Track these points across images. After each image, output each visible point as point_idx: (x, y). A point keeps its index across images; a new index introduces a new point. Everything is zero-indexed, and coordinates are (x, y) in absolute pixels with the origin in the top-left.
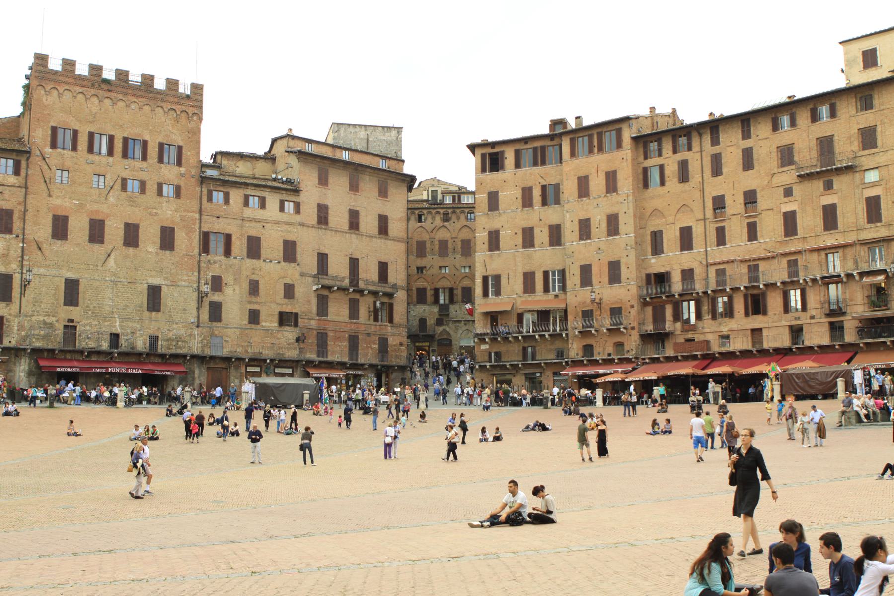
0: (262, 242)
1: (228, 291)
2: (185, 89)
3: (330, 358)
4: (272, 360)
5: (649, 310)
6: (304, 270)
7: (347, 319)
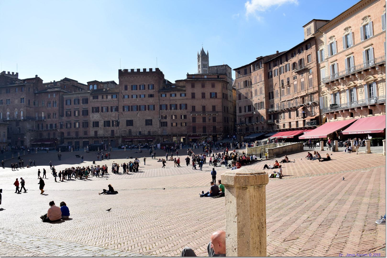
1: (167, 118)
2: (154, 70)
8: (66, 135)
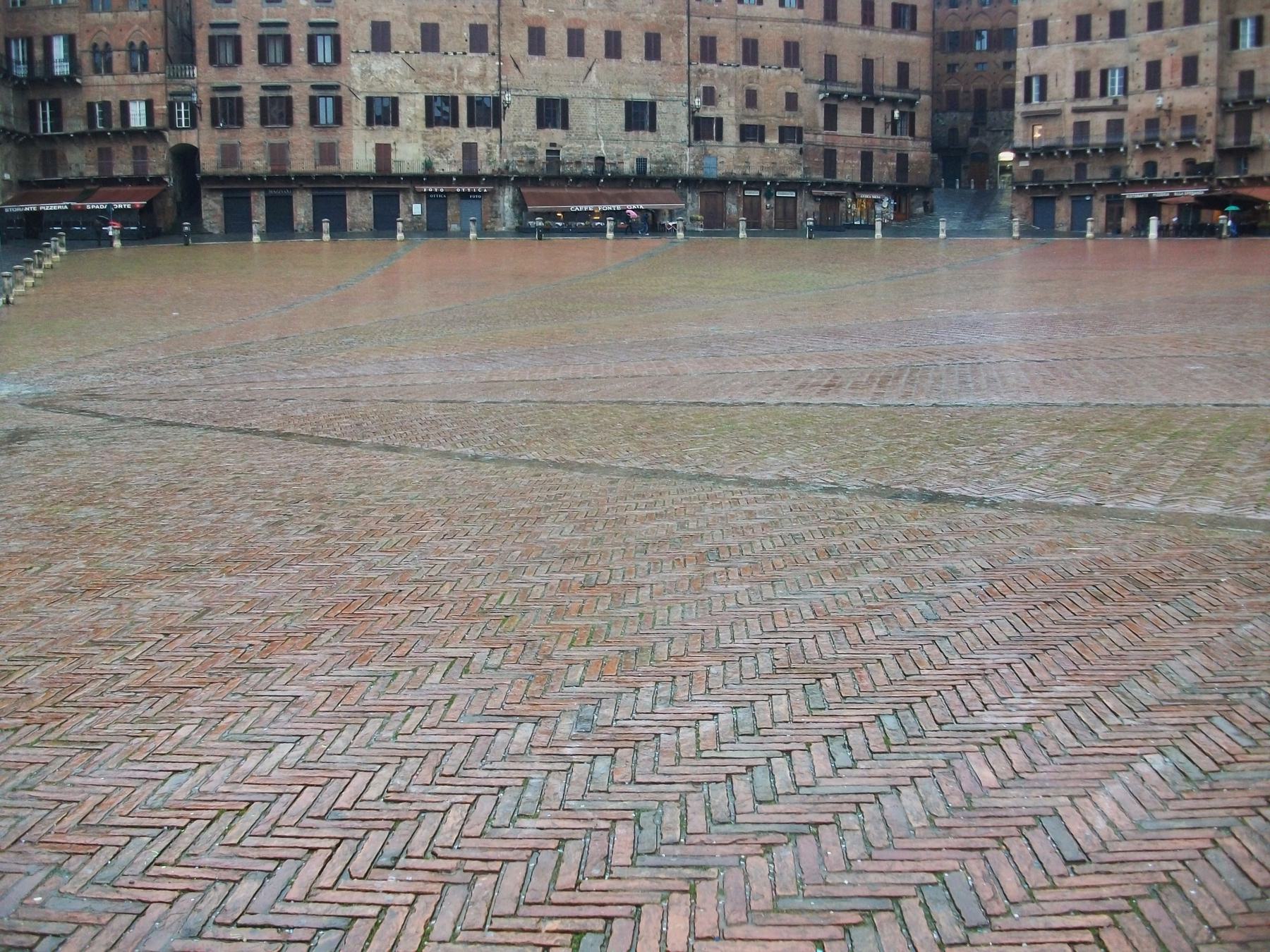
0: (760, 44)
1: (723, 104)
3: (839, 178)
4: (773, 182)
5: (1231, 120)
6: (810, 76)
7: (859, 132)
8: (209, 162)
